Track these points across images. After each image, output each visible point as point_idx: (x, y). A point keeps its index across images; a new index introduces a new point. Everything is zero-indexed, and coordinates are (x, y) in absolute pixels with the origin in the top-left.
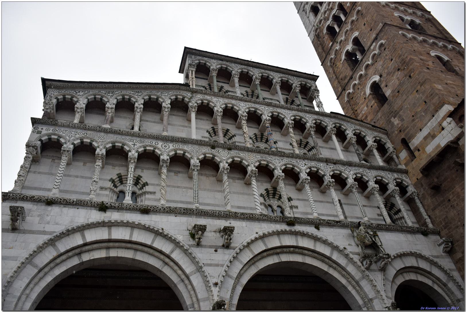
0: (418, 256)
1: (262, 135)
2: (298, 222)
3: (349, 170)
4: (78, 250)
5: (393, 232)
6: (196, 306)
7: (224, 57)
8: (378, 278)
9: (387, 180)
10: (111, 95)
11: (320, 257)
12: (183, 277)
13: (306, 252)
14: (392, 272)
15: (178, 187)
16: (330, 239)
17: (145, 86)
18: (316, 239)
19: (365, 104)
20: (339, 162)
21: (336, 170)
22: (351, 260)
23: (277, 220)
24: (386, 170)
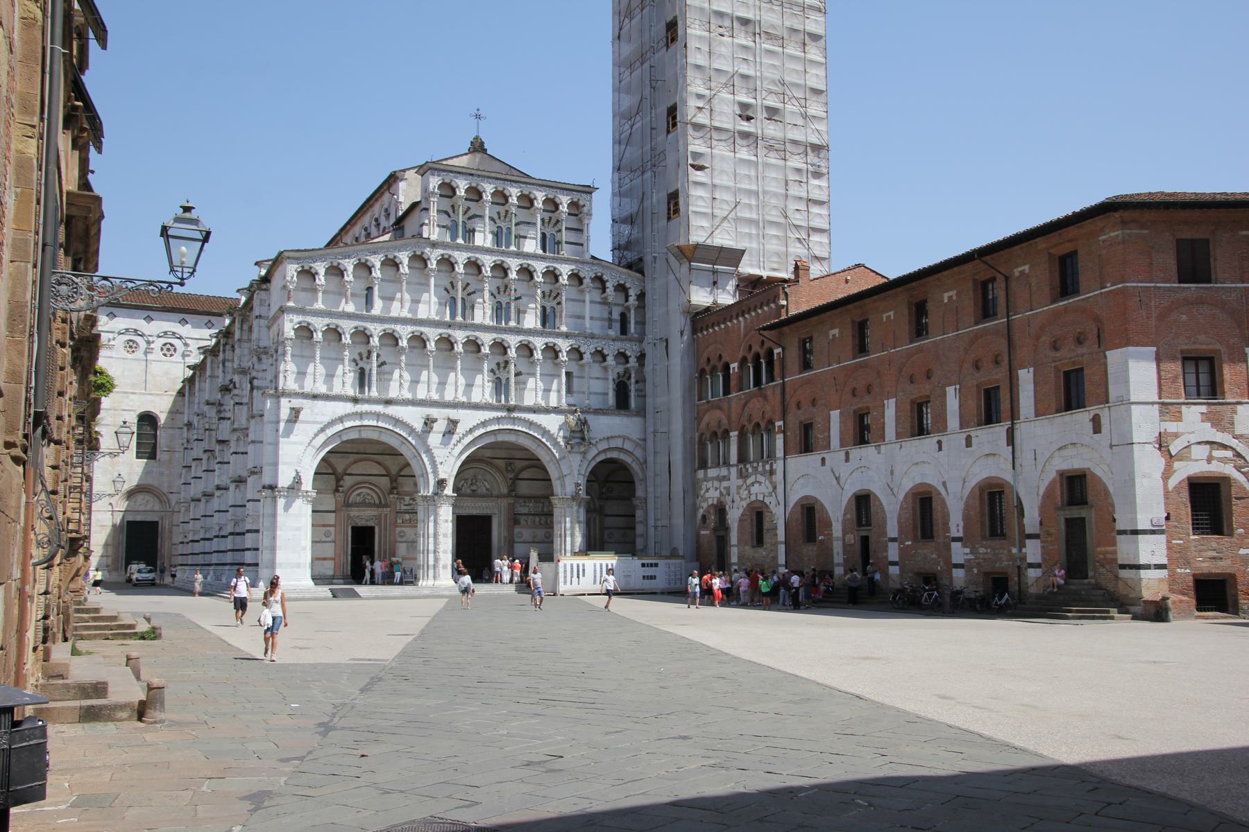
0: (625, 438)
1: (506, 287)
4: (339, 433)
6: (425, 476)
8: (576, 459)
10: (347, 260)
12: (416, 454)
14: (593, 452)
15: (413, 365)
16: (544, 424)
18: (531, 424)
22: (556, 444)
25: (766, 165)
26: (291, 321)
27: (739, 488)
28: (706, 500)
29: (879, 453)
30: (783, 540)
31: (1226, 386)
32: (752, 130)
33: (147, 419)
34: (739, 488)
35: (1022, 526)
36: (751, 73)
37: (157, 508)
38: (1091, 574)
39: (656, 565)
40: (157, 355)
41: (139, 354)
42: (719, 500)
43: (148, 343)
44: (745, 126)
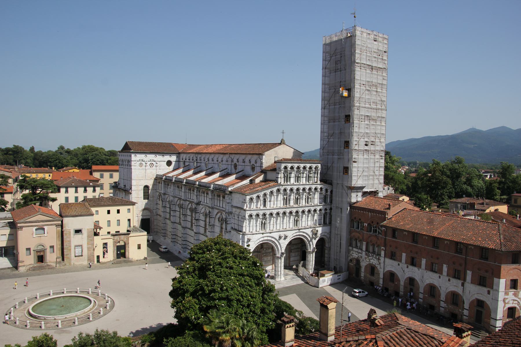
18: (304, 232)
25: (371, 158)
26: (248, 214)
27: (366, 258)
28: (353, 256)
29: (419, 270)
30: (382, 278)
31: (518, 287)
32: (368, 149)
33: (146, 187)
34: (366, 258)
35: (463, 306)
36: (368, 132)
37: (149, 214)
38: (482, 324)
39: (340, 275)
40: (148, 167)
41: (144, 167)
42: (357, 258)
43: (146, 163)
44: (366, 148)
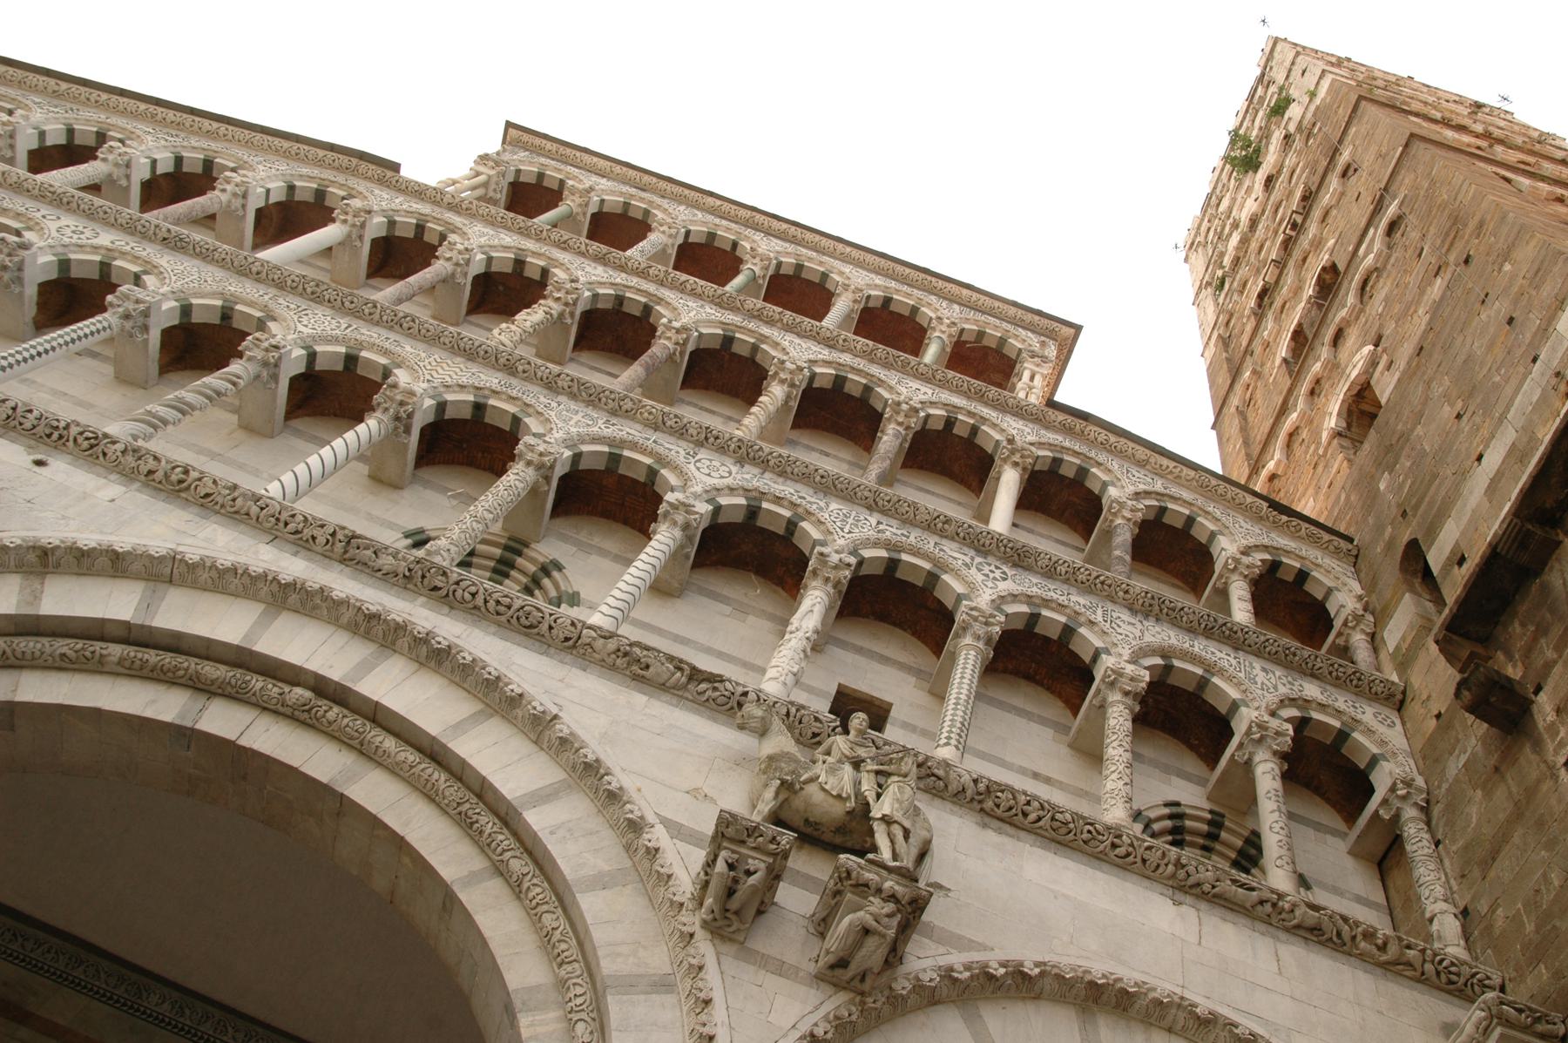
2: (436, 589)
3: (998, 574)
5: (1105, 866)
7: (655, 180)
9: (1239, 684)
11: (453, 791)
13: (390, 743)
17: (215, 125)
19: (1311, 491)
20: (950, 529)
21: (916, 552)
23: (314, 538)
24: (1259, 652)
